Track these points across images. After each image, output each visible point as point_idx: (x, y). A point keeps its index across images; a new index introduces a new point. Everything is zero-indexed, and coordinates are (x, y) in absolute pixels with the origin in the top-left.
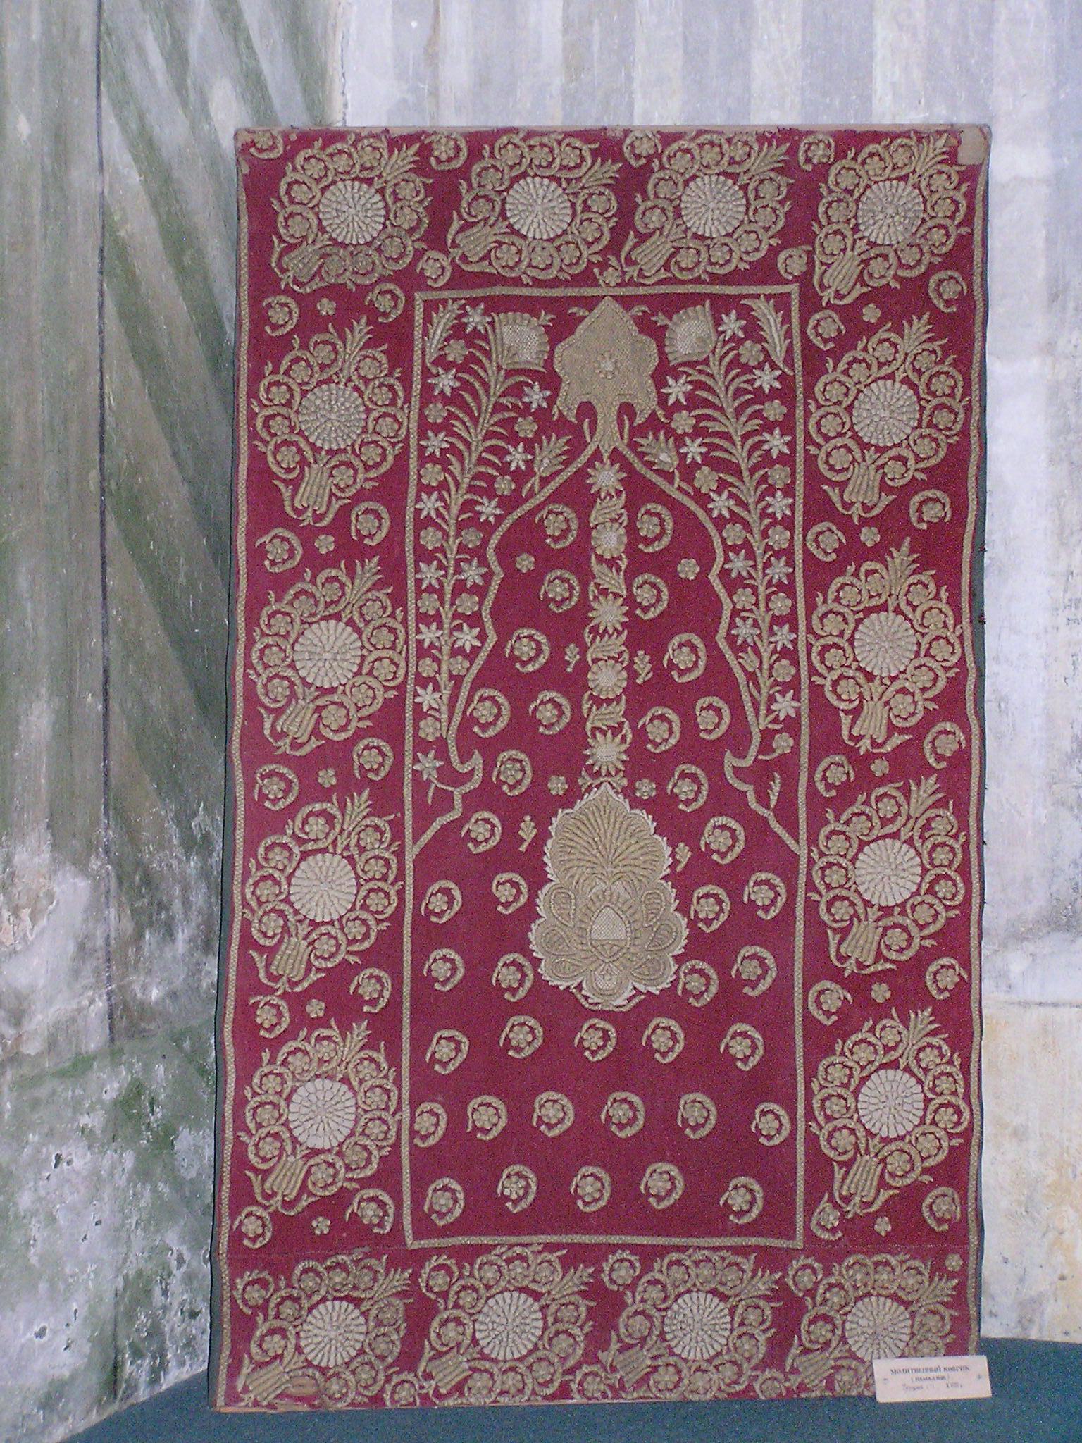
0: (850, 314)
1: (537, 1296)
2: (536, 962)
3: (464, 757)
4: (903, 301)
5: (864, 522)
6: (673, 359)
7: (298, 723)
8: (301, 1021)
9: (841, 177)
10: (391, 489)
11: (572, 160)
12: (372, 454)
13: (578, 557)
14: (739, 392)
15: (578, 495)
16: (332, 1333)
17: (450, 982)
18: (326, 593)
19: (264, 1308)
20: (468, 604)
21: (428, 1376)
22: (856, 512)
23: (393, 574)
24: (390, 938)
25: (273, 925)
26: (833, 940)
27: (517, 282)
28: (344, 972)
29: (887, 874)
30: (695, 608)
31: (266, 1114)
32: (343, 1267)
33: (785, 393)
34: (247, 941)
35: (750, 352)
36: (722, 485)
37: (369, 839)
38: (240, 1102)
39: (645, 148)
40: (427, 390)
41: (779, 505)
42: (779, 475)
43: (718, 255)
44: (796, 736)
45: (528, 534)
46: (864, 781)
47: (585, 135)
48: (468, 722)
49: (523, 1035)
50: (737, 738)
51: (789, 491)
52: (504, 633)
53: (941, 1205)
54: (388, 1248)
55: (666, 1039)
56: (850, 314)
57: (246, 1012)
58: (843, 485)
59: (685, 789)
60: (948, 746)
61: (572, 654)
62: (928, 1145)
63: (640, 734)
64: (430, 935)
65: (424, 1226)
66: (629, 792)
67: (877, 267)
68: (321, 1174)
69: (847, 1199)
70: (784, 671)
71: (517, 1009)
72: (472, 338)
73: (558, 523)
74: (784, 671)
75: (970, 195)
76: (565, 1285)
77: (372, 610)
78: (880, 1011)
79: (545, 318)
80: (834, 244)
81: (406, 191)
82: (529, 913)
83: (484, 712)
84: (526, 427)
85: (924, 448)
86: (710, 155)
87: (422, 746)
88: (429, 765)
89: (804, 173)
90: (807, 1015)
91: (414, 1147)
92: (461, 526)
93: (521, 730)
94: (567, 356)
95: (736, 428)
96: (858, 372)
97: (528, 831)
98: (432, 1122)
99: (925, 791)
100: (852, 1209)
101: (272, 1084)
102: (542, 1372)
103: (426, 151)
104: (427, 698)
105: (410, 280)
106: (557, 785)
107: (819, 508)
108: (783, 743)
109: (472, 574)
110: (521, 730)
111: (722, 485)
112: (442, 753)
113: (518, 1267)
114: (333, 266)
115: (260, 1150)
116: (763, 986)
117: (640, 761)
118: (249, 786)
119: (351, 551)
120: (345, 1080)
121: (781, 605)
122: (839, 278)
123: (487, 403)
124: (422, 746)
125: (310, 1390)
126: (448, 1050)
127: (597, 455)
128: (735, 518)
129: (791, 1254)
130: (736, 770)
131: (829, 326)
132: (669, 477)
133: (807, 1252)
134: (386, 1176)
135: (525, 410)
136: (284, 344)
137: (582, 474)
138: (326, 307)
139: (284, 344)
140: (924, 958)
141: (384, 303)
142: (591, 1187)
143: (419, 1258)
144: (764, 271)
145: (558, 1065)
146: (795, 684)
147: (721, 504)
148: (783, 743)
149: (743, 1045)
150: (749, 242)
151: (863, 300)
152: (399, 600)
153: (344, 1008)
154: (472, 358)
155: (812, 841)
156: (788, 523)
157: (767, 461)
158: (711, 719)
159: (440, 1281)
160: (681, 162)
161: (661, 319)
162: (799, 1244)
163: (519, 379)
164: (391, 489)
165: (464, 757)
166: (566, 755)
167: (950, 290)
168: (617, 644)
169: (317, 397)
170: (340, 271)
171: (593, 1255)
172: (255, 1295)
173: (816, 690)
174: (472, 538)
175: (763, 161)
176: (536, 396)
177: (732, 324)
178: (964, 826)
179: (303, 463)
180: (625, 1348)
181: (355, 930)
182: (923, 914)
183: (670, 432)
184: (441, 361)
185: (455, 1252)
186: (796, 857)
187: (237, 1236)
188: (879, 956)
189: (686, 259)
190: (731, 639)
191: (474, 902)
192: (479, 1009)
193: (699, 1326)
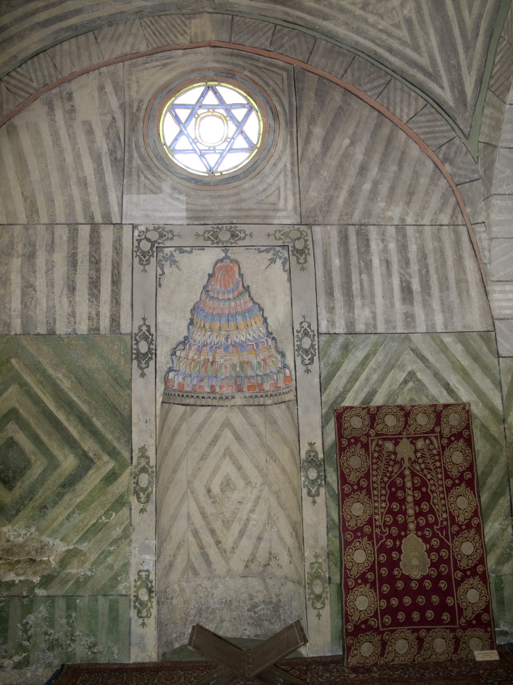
0: (449, 439)
1: (407, 640)
2: (401, 570)
3: (385, 529)
4: (458, 436)
5: (456, 479)
6: (418, 449)
7: (352, 523)
8: (357, 584)
9: (445, 413)
10: (367, 476)
11: (396, 411)
12: (363, 469)
13: (403, 488)
14: (430, 455)
15: (402, 476)
16: (366, 649)
17: (385, 574)
18: (357, 497)
19: (353, 644)
20: (383, 498)
21: (386, 658)
22: (454, 477)
23: (369, 493)
24: (373, 566)
25: (350, 564)
26: (458, 562)
27: (388, 435)
28: (365, 573)
29: (467, 548)
30: (426, 497)
31: (351, 603)
32: (368, 635)
33: (439, 454)
34: (346, 568)
35: (431, 447)
36: (429, 473)
37: (368, 546)
38: (346, 601)
39: (409, 408)
40: (373, 457)
41: (440, 476)
42: (439, 470)
43: (424, 428)
44: (447, 521)
45: (393, 484)
46: (461, 530)
47: (398, 406)
48: (385, 521)
49: (400, 585)
50: (436, 522)
51: (441, 473)
52: (390, 504)
53: (485, 617)
54: (377, 630)
55: (428, 584)
56: (449, 439)
57: (346, 583)
58: (451, 472)
59: (427, 533)
60: (476, 522)
61: (403, 507)
62: (481, 604)
63: (418, 523)
64: (381, 565)
65: (383, 626)
66: (416, 534)
67: (453, 430)
68: (363, 615)
69: (466, 617)
70: (444, 509)
71: (399, 579)
72: (380, 446)
73: (399, 481)
74: (444, 509)
75: (468, 415)
76: (412, 637)
77: (365, 500)
78: (469, 577)
79: (393, 442)
80: (445, 425)
81: (366, 418)
82: (399, 560)
83: (388, 519)
84: (392, 463)
85: (465, 464)
86: (420, 409)
87: (377, 527)
88: (378, 530)
89: (438, 412)
90: (455, 578)
91: (380, 610)
92: (381, 483)
93: (395, 523)
94: (398, 448)
95: (430, 461)
96: (451, 449)
97: (398, 543)
98: (384, 604)
99: (473, 531)
100: (468, 619)
101: (352, 597)
102: (409, 656)
103: (369, 410)
104: (377, 517)
105: (368, 435)
106: (403, 533)
107: (447, 477)
108: (445, 523)
109: (384, 492)
110: (395, 523)
111: (429, 473)
112: (381, 528)
113: (403, 634)
114: (353, 433)
115: (350, 611)
116: (446, 572)
117: (419, 528)
118: (344, 536)
119: (361, 488)
120: (366, 596)
121: (442, 496)
122: (446, 432)
123: (384, 458)
124: (377, 527)
125: (363, 661)
126: (386, 588)
127: (405, 468)
128: (432, 479)
129: (457, 629)
130: (437, 529)
131: (445, 441)
132: (419, 472)
133: (460, 628)
134: (375, 615)
135: (391, 460)
136: (345, 448)
137: (403, 472)
138: (353, 441)
139: (345, 448)
140: (476, 566)
141: (363, 440)
142: (416, 616)
143: (383, 632)
144: (432, 431)
145: (407, 591)
146: (446, 511)
147: (429, 476)
148: (445, 523)
149: (443, 585)
150: (429, 426)
151: (451, 436)
152: (370, 498)
153: (365, 581)
154: (380, 450)
155: (452, 542)
156: (442, 480)
157: (437, 468)
158: (431, 519)
159: (387, 637)
160: (415, 411)
161: (414, 441)
162: (458, 626)
163: (389, 453)
164: (367, 476)
165: (385, 529)
166: (404, 527)
167: (467, 433)
168: (412, 505)
169: (352, 459)
170: (355, 434)
171: (418, 630)
172: (351, 642)
173: (450, 512)
174: (383, 485)
175: (430, 410)
176: (393, 457)
177: (428, 442)
178: (481, 538)
179: (350, 471)
180: (425, 650)
181: (366, 565)
182: (475, 556)
183: (418, 463)
184: (375, 451)
185: (389, 631)
186: (449, 546)
187: (347, 629)
188: (467, 566)
189: (418, 430)
190: (433, 503)
191: (388, 558)
192: (391, 580)
193: (440, 645)
